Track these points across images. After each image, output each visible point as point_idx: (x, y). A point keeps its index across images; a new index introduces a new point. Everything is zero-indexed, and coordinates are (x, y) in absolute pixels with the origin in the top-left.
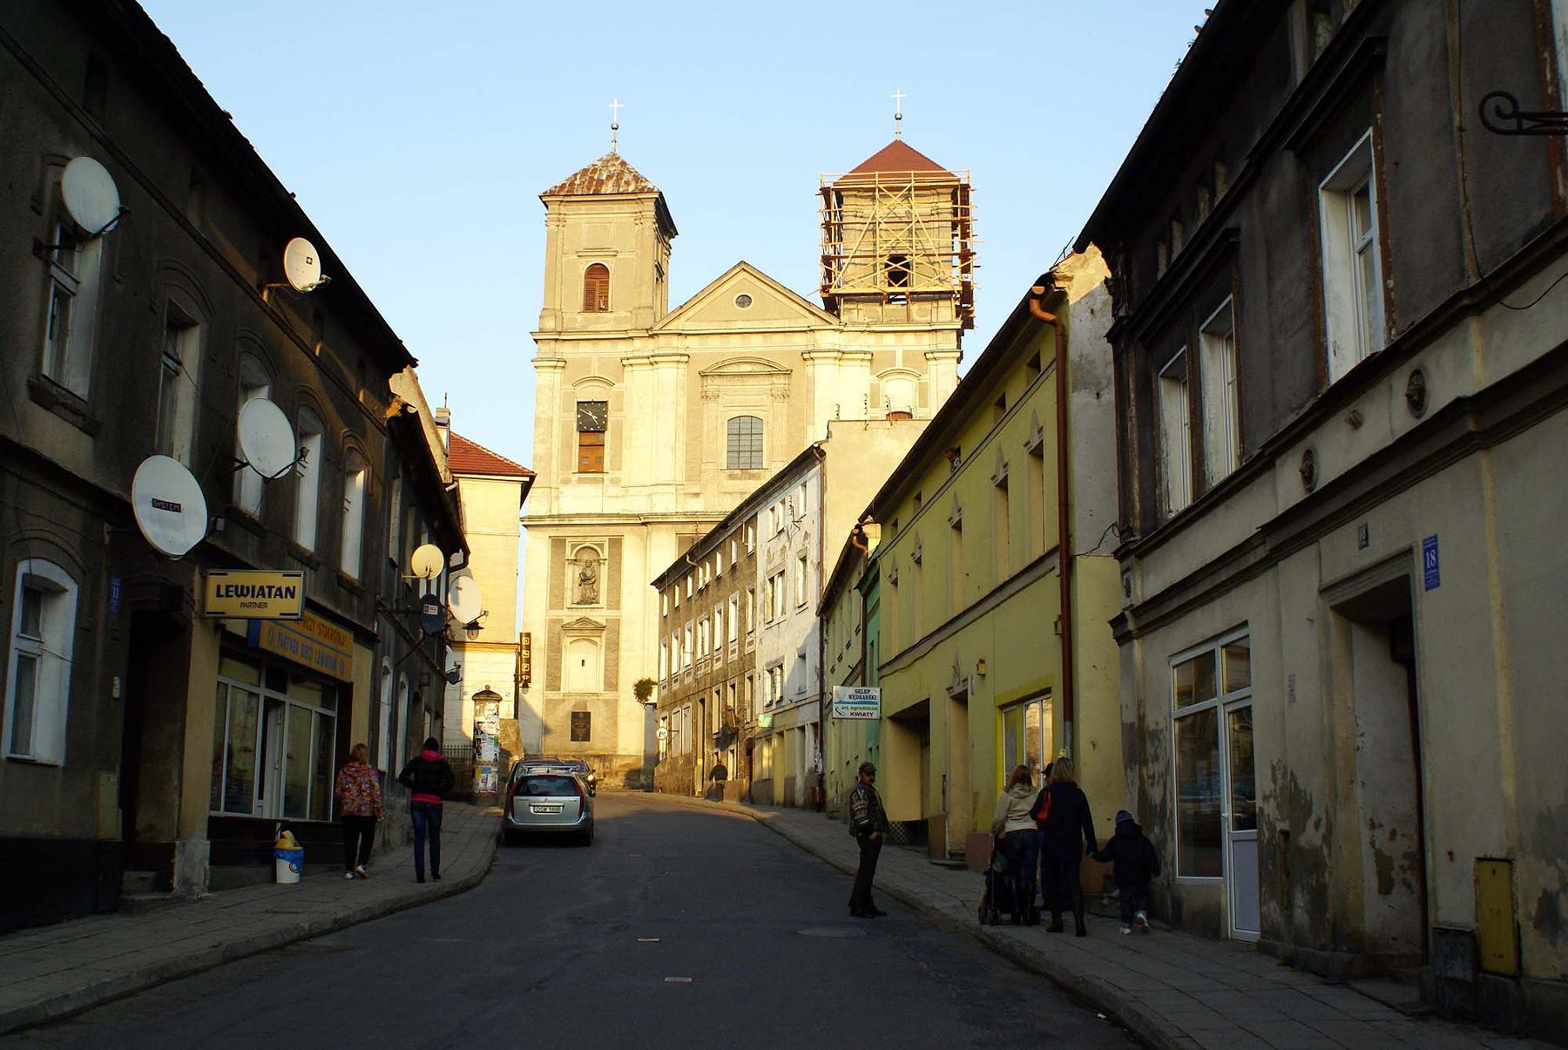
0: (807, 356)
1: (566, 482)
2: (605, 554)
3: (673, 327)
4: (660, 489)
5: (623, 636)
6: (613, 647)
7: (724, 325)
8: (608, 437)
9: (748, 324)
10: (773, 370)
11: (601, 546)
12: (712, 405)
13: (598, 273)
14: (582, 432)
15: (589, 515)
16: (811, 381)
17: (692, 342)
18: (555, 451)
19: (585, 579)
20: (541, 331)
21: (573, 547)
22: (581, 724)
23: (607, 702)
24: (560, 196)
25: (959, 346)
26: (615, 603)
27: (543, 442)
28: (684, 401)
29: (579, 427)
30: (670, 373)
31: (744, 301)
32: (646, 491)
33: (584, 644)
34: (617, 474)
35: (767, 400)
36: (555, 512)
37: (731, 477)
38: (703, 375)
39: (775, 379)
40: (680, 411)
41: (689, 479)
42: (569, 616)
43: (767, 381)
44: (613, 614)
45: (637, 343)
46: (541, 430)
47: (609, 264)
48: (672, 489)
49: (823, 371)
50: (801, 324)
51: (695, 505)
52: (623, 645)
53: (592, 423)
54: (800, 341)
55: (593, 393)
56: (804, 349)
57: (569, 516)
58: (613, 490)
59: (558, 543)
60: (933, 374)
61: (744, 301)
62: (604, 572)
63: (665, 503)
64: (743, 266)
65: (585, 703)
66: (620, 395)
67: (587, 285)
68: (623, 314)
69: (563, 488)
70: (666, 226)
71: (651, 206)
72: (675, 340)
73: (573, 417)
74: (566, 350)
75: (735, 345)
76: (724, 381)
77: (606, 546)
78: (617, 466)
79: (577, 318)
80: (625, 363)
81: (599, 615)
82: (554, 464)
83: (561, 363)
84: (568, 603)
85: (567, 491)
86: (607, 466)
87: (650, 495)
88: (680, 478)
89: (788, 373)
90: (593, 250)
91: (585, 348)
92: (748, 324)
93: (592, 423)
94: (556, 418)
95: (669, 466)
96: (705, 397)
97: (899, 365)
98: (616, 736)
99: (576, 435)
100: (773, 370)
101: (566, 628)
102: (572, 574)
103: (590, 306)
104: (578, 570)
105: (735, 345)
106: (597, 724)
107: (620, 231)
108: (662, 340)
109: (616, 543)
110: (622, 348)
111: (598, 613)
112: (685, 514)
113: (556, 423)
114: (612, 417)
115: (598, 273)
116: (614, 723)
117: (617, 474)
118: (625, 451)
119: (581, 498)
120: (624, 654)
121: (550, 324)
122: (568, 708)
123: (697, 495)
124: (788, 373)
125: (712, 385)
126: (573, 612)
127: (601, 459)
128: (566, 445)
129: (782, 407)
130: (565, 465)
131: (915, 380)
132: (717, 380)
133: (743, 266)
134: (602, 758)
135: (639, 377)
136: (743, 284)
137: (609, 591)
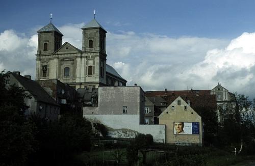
0: (76, 57)
16: (77, 61)
17: (59, 56)
50: (75, 52)
55: (45, 64)
75: (66, 56)
78: (48, 76)
79: (43, 52)
89: (73, 60)
91: (44, 57)
96: (61, 64)
103: (44, 50)
110: (49, 57)
115: (46, 44)
124: (73, 60)
125: (62, 62)
135: (51, 61)
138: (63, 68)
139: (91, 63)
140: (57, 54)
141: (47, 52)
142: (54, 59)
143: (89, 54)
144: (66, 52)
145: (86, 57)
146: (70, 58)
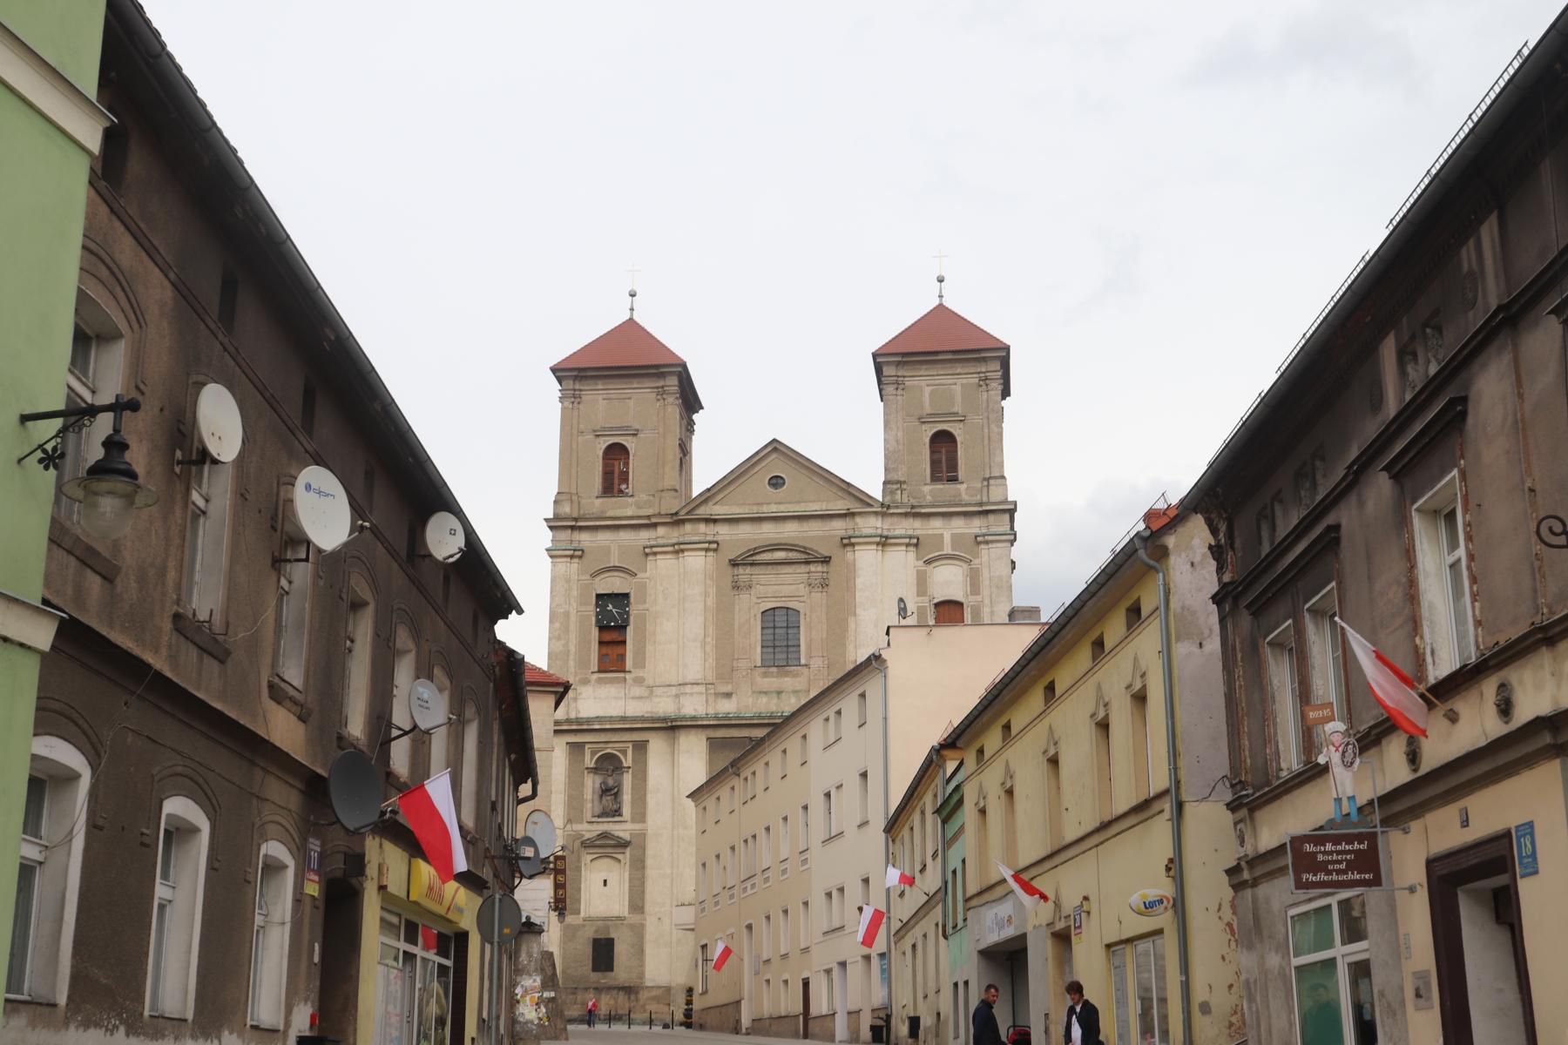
0: (847, 543)
1: (585, 682)
2: (628, 761)
3: (703, 511)
4: (688, 689)
5: (649, 852)
6: (639, 865)
7: (755, 509)
8: (630, 631)
9: (782, 508)
10: (810, 557)
11: (624, 752)
12: (744, 596)
13: (616, 453)
14: (602, 629)
15: (611, 719)
16: (851, 571)
17: (723, 531)
18: (572, 648)
19: (605, 791)
20: (557, 517)
21: (593, 753)
22: (603, 953)
23: (632, 927)
24: (575, 375)
25: (1012, 528)
26: (640, 815)
27: (559, 638)
28: (712, 591)
29: (598, 621)
30: (696, 561)
31: (776, 482)
32: (674, 691)
33: (606, 861)
34: (640, 673)
35: (802, 589)
36: (573, 716)
37: (765, 675)
38: (734, 564)
39: (812, 568)
40: (710, 602)
41: (720, 677)
42: (590, 830)
43: (804, 568)
44: (638, 826)
45: (661, 531)
46: (557, 625)
47: (629, 443)
48: (702, 689)
49: (866, 558)
50: (840, 505)
51: (727, 707)
52: (649, 862)
54: (839, 527)
55: (613, 584)
56: (842, 533)
57: (589, 721)
58: (637, 691)
59: (577, 749)
60: (985, 559)
61: (776, 482)
62: (627, 780)
63: (694, 706)
64: (775, 447)
65: (607, 928)
66: (644, 585)
67: (605, 465)
68: (644, 497)
70: (690, 402)
71: (672, 382)
72: (702, 527)
73: (591, 610)
74: (585, 539)
75: (769, 532)
76: (756, 570)
77: (630, 752)
78: (640, 663)
79: (596, 504)
80: (649, 552)
81: (622, 829)
82: (571, 663)
83: (577, 554)
84: (588, 816)
86: (629, 664)
87: (677, 696)
88: (710, 677)
89: (826, 560)
90: (611, 429)
91: (603, 537)
92: (782, 508)
94: (573, 611)
95: (696, 665)
96: (736, 587)
97: (948, 550)
98: (642, 964)
99: (595, 632)
100: (810, 557)
101: (587, 845)
102: (591, 783)
104: (599, 779)
105: (769, 532)
106: (621, 951)
107: (638, 407)
108: (688, 527)
109: (641, 747)
110: (645, 536)
111: (623, 826)
112: (716, 718)
113: (573, 619)
114: (634, 609)
115: (616, 453)
116: (640, 952)
117: (640, 673)
118: (649, 648)
119: (595, 701)
120: (651, 873)
121: (566, 509)
122: (589, 933)
123: (728, 695)
124: (826, 560)
126: (595, 827)
127: (622, 657)
129: (817, 596)
130: (583, 663)
131: (965, 566)
132: (748, 570)
133: (775, 447)
134: (629, 990)
135: (664, 565)
136: (777, 467)
137: (633, 802)
138: (749, 609)
140: (707, 521)
141: (623, 508)
142: (678, 550)
143: (937, 523)
144: (772, 509)
145: (915, 543)
146: (804, 551)
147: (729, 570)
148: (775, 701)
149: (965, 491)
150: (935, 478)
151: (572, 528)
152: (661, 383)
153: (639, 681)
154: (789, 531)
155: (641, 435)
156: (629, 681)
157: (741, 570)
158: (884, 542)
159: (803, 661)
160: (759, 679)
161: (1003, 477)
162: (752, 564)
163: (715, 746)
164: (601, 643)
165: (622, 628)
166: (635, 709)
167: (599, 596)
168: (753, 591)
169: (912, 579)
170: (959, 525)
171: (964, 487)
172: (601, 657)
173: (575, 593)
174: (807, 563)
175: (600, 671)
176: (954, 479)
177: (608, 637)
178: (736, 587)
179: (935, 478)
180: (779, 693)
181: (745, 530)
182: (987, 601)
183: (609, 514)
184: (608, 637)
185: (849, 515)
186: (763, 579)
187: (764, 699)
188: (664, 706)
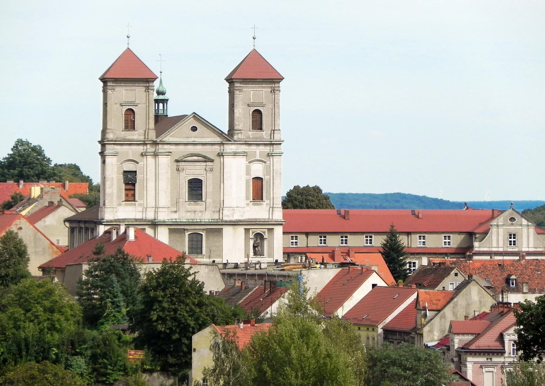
0: (220, 155)
1: (120, 205)
8: (137, 185)
10: (207, 160)
14: (126, 184)
17: (173, 147)
31: (194, 129)
37: (189, 205)
38: (177, 161)
43: (204, 164)
48: (166, 209)
49: (228, 160)
51: (175, 217)
53: (130, 180)
55: (130, 167)
58: (141, 209)
61: (194, 129)
69: (119, 207)
73: (121, 177)
75: (191, 149)
78: (142, 198)
85: (121, 208)
89: (212, 161)
93: (130, 180)
95: (165, 200)
97: (258, 158)
99: (123, 186)
100: (207, 160)
105: (191, 149)
114: (139, 177)
117: (142, 202)
123: (176, 212)
124: (212, 161)
127: (134, 195)
128: (119, 189)
130: (119, 197)
132: (183, 163)
139: (258, 170)
143: (254, 147)
144: (191, 140)
145: (245, 154)
146: (204, 157)
147: (176, 164)
148: (193, 215)
149: (265, 134)
150: (254, 128)
151: (114, 144)
152: (148, 85)
153: (140, 205)
154: (198, 149)
155: (139, 106)
156: (137, 205)
157: (180, 164)
158: (235, 154)
159: (203, 200)
160: (187, 206)
161: (279, 130)
162: (185, 161)
163: (171, 231)
164: (126, 190)
165: (134, 185)
166: (139, 216)
167: (125, 172)
168: (184, 171)
169: (244, 169)
170: (262, 148)
171: (264, 132)
172: (127, 195)
173: (116, 170)
174: (205, 161)
175: (126, 201)
176: (261, 129)
177: (128, 187)
178: (178, 170)
179: (254, 128)
180: (195, 212)
181: (181, 147)
182: (272, 178)
183: (128, 138)
184: (128, 187)
185: (222, 144)
186: (189, 167)
187: (189, 214)
188: (150, 216)
